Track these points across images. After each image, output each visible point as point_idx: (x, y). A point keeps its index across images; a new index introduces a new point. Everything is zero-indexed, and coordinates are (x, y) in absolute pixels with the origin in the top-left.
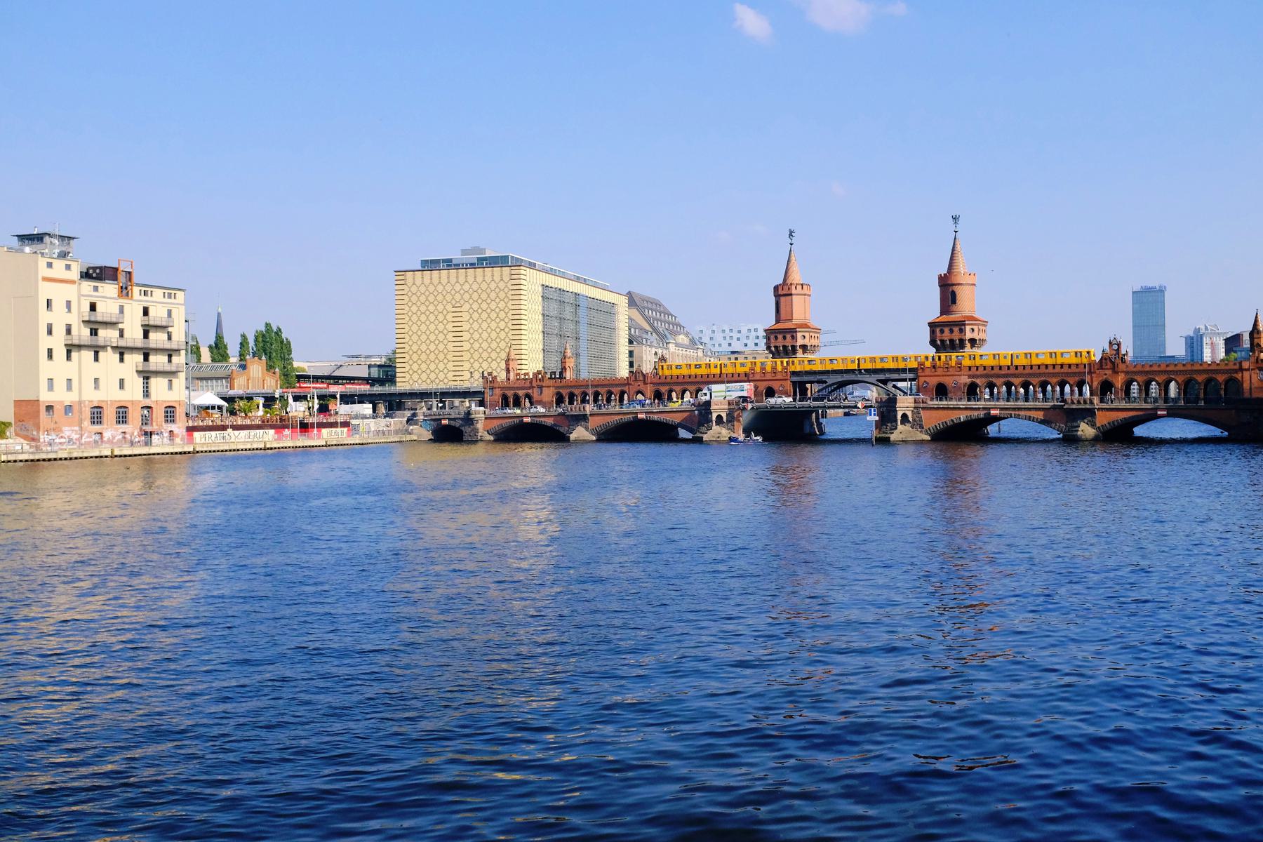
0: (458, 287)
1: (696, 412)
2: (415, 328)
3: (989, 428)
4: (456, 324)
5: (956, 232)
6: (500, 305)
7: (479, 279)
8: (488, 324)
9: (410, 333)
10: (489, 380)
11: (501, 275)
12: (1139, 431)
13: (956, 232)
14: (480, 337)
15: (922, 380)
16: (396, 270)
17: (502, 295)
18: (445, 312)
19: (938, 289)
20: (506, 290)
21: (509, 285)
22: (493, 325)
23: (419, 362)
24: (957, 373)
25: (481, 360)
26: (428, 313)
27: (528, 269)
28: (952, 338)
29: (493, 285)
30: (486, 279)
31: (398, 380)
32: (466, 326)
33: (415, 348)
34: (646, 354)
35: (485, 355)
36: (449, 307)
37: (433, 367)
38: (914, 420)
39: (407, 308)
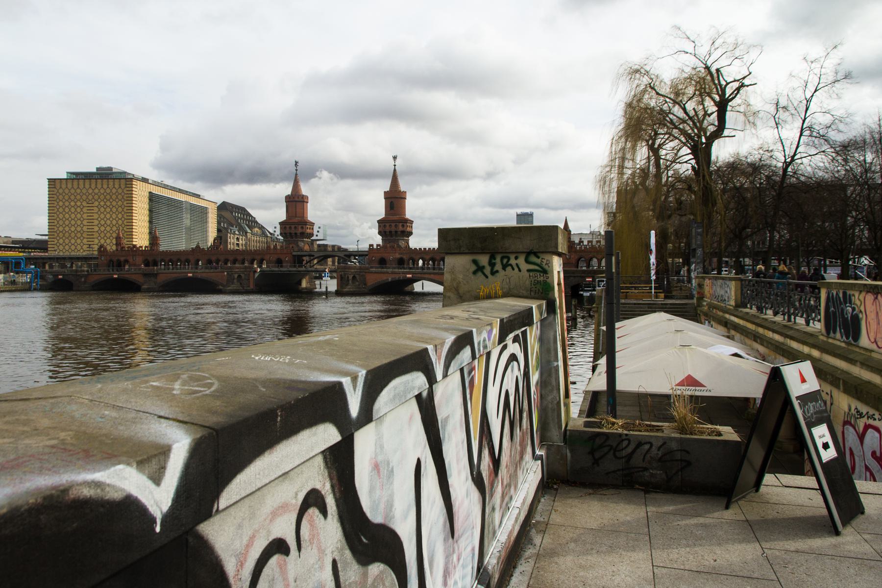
0: (90, 191)
1: (226, 273)
2: (61, 216)
3: (415, 284)
4: (89, 214)
7: (105, 186)
9: (58, 219)
10: (102, 249)
14: (105, 223)
17: (120, 197)
19: (383, 201)
25: (105, 238)
26: (70, 206)
27: (138, 182)
29: (114, 191)
30: (110, 186)
31: (49, 249)
32: (96, 216)
33: (61, 229)
34: (230, 238)
35: (108, 235)
36: (84, 204)
39: (56, 203)
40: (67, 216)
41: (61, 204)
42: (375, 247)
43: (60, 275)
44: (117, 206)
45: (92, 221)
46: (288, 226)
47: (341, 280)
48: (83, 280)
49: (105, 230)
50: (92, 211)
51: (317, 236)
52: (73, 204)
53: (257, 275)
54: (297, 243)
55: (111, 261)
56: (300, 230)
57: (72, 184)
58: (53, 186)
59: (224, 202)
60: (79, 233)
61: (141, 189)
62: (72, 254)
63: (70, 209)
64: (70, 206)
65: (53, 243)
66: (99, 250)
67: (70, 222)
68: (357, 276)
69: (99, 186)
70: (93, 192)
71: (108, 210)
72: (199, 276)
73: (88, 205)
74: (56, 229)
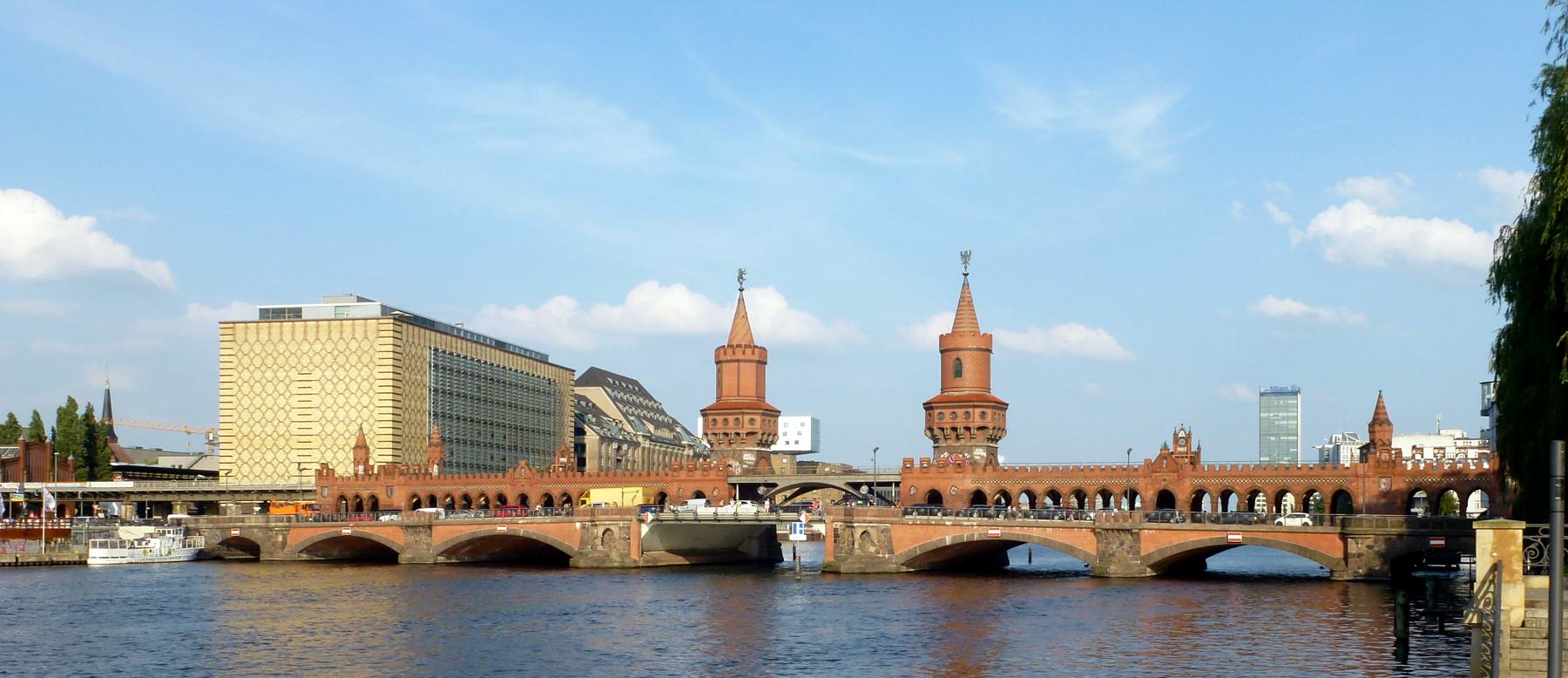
1: (578, 525)
4: (302, 398)
5: (966, 275)
6: (362, 373)
7: (335, 336)
8: (347, 398)
10: (325, 473)
11: (366, 331)
12: (1214, 563)
13: (966, 275)
14: (335, 416)
15: (908, 483)
16: (221, 321)
17: (365, 359)
18: (287, 381)
19: (940, 355)
20: (371, 352)
21: (375, 345)
22: (353, 400)
23: (251, 449)
24: (956, 475)
26: (264, 381)
27: (405, 325)
28: (955, 425)
29: (354, 345)
30: (345, 335)
33: (246, 429)
36: (294, 375)
37: (269, 456)
38: (878, 542)
39: (236, 375)
40: (258, 402)
41: (246, 375)
42: (917, 464)
43: (235, 528)
44: (359, 380)
45: (308, 411)
46: (720, 419)
47: (835, 541)
48: (280, 538)
49: (335, 430)
50: (309, 391)
51: (797, 442)
52: (269, 374)
53: (645, 529)
54: (741, 455)
55: (342, 497)
56: (748, 428)
57: (270, 334)
58: (230, 338)
59: (592, 368)
60: (281, 439)
61: (411, 340)
62: (267, 483)
63: (263, 387)
64: (264, 381)
65: (228, 460)
66: (319, 473)
67: (264, 414)
68: (872, 531)
69: (323, 336)
70: (311, 348)
71: (341, 387)
72: (521, 533)
73: (301, 377)
74: (236, 430)
